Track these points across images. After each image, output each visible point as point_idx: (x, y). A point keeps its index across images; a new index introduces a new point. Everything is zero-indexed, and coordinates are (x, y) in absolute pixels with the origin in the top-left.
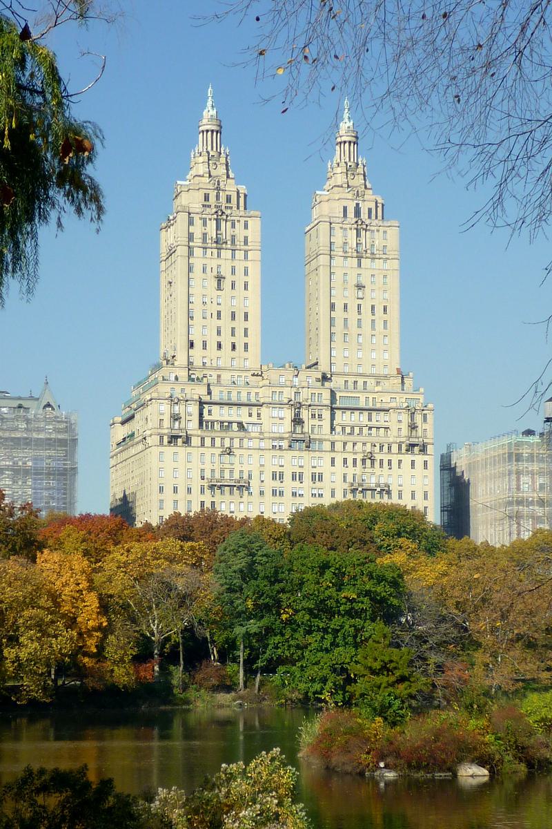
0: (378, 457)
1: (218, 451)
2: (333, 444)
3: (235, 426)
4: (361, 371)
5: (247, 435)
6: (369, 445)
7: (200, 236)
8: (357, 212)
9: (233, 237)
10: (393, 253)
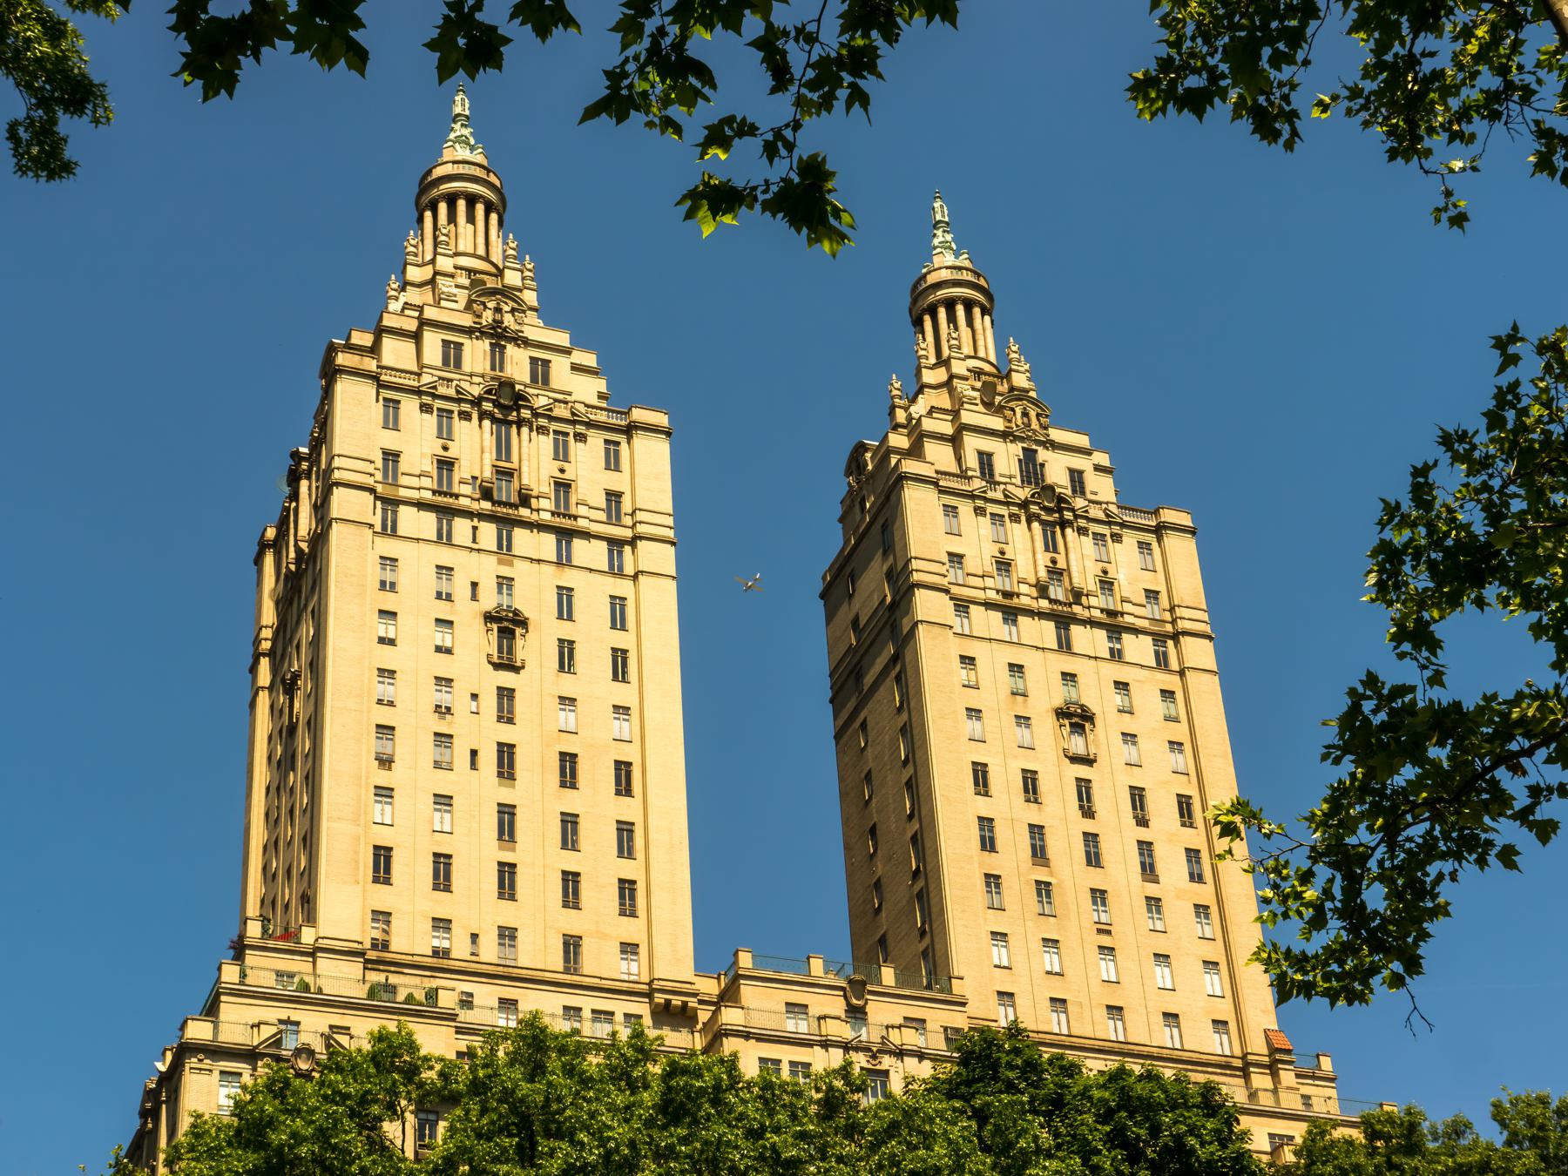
9: (563, 486)
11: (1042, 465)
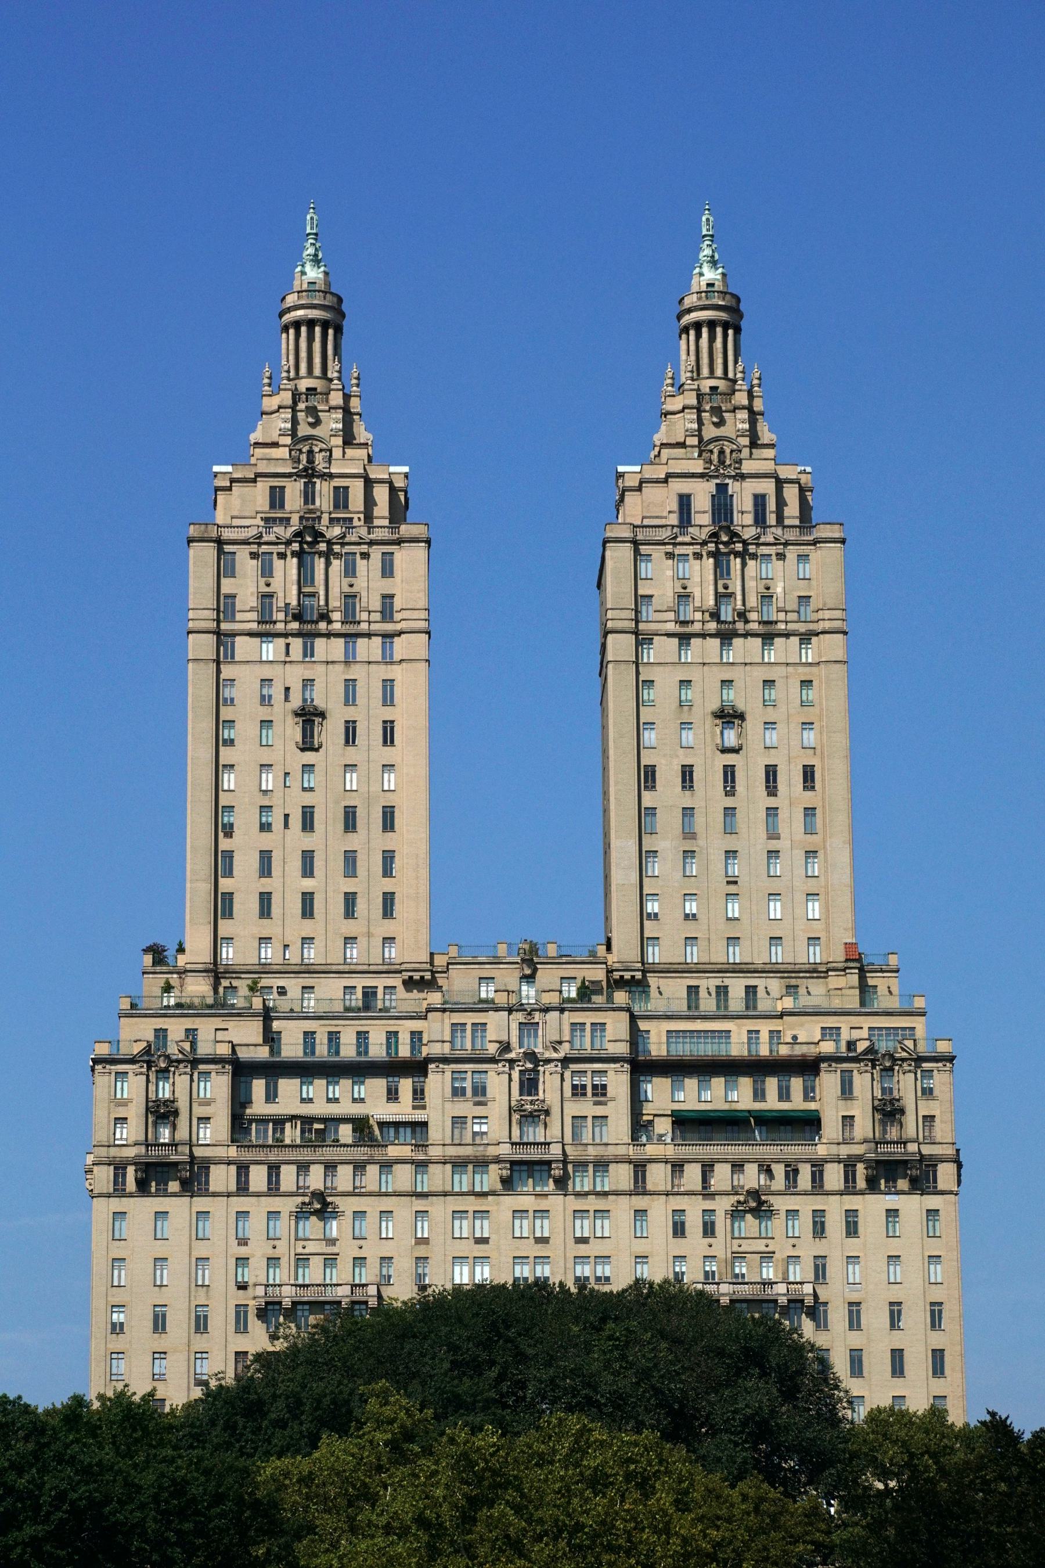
0: (781, 1204)
1: (287, 1206)
2: (640, 1167)
3: (346, 1133)
4: (736, 955)
5: (377, 1154)
6: (751, 1169)
7: (253, 602)
9: (350, 598)
10: (827, 614)
11: (732, 496)
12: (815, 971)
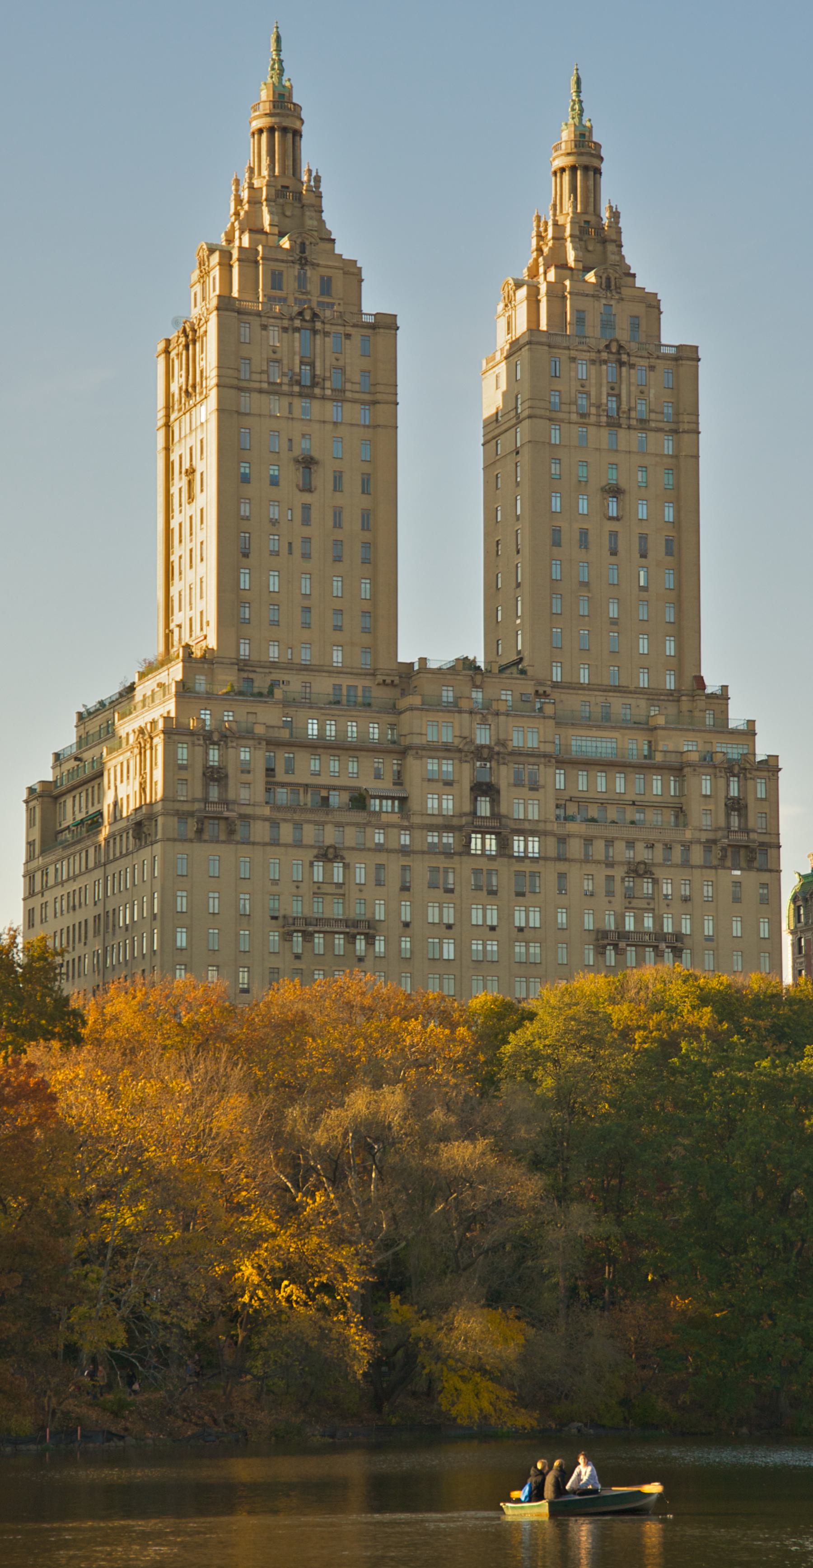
6: (640, 846)
8: (608, 324)
12: (672, 695)
